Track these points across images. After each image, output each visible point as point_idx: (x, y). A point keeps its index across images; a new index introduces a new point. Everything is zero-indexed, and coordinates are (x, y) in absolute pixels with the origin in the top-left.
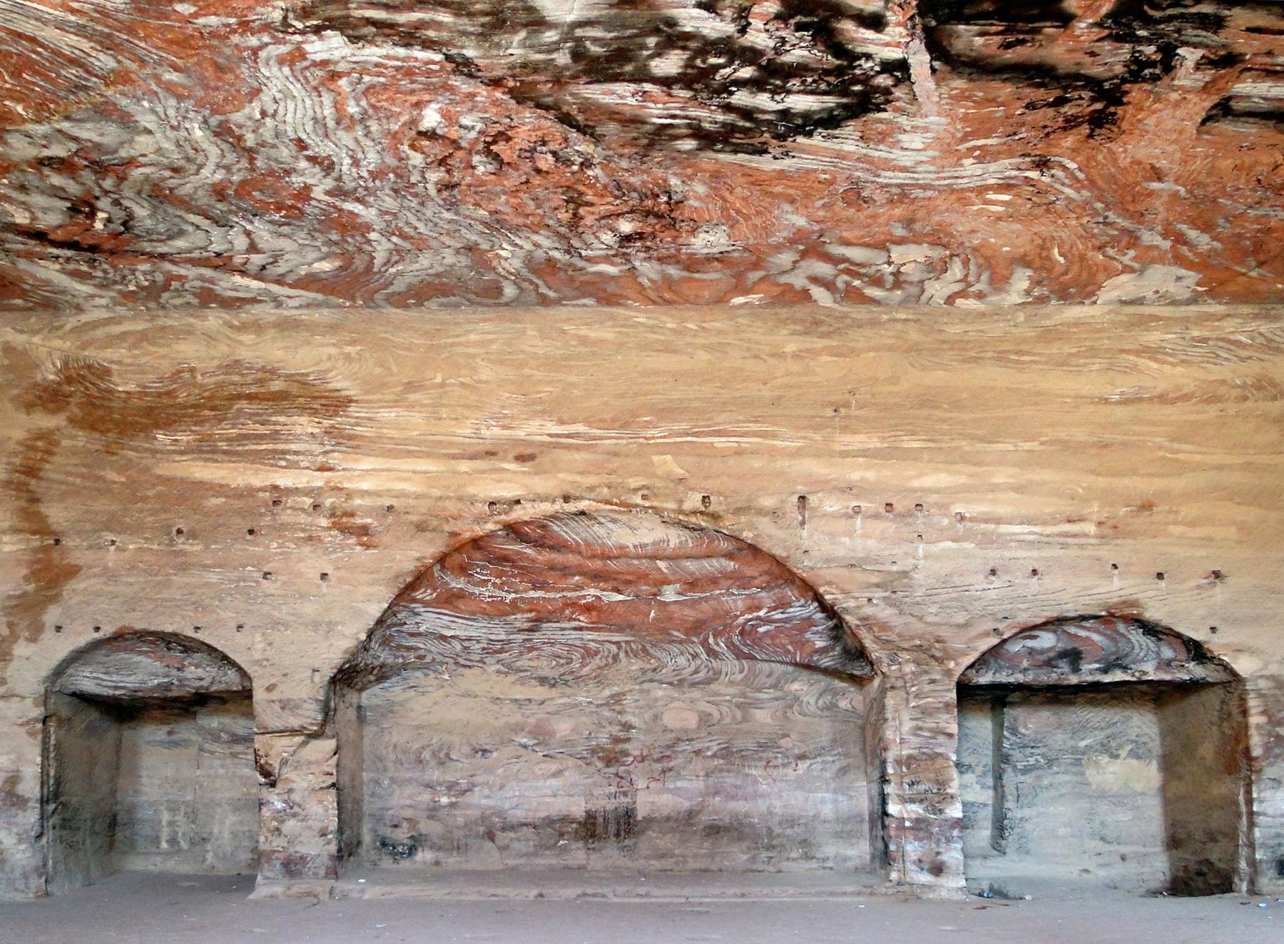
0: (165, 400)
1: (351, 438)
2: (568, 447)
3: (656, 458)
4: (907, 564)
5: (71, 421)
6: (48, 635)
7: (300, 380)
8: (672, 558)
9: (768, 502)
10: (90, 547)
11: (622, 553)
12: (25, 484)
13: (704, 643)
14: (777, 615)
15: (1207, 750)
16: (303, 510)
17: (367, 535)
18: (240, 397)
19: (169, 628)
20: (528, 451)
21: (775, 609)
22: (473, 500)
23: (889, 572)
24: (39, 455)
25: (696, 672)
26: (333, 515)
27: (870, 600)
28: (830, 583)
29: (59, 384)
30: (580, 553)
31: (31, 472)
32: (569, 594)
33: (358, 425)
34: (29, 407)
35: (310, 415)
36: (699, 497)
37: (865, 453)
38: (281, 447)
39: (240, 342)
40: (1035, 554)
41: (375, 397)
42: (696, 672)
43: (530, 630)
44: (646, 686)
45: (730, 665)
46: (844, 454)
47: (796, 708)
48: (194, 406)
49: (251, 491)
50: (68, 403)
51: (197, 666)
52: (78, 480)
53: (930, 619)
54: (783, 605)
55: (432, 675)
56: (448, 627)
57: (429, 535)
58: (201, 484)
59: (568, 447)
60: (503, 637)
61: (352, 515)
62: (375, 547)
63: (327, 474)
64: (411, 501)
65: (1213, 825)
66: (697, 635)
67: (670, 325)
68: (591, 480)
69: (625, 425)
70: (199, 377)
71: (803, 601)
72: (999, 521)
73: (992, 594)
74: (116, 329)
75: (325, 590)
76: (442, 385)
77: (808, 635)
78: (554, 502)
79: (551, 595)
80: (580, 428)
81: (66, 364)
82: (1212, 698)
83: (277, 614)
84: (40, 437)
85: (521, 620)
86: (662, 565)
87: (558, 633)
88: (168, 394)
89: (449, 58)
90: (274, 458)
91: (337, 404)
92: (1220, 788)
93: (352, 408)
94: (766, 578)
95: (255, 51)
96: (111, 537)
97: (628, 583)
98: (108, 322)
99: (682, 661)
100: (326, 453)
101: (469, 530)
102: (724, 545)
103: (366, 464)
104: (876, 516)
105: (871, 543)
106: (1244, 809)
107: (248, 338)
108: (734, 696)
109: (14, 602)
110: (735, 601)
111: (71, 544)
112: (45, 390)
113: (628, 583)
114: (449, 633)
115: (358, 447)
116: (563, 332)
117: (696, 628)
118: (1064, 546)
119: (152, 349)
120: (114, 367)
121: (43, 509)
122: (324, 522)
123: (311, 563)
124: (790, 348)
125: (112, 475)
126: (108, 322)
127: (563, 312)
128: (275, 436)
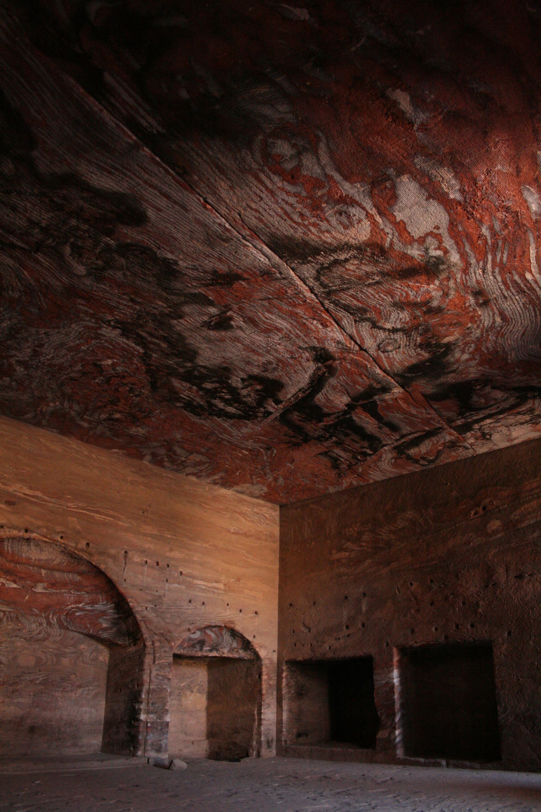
2: (32, 503)
3: (69, 518)
4: (161, 592)
8: (52, 569)
9: (113, 551)
11: (28, 562)
13: (47, 618)
14: (88, 608)
23: (155, 595)
25: (39, 633)
27: (146, 608)
28: (132, 597)
30: (6, 558)
37: (151, 536)
42: (39, 633)
44: (13, 639)
45: (56, 631)
47: (81, 658)
53: (167, 620)
54: (93, 603)
59: (32, 503)
66: (45, 612)
67: (86, 453)
68: (40, 523)
73: (189, 612)
77: (100, 620)
78: (20, 531)
80: (39, 494)
86: (43, 572)
89: (145, 354)
99: (34, 626)
102: (83, 568)
104: (152, 567)
105: (149, 580)
106: (256, 717)
108: (54, 649)
110: (69, 596)
117: (46, 608)
124: (129, 479)
127: (41, 431)
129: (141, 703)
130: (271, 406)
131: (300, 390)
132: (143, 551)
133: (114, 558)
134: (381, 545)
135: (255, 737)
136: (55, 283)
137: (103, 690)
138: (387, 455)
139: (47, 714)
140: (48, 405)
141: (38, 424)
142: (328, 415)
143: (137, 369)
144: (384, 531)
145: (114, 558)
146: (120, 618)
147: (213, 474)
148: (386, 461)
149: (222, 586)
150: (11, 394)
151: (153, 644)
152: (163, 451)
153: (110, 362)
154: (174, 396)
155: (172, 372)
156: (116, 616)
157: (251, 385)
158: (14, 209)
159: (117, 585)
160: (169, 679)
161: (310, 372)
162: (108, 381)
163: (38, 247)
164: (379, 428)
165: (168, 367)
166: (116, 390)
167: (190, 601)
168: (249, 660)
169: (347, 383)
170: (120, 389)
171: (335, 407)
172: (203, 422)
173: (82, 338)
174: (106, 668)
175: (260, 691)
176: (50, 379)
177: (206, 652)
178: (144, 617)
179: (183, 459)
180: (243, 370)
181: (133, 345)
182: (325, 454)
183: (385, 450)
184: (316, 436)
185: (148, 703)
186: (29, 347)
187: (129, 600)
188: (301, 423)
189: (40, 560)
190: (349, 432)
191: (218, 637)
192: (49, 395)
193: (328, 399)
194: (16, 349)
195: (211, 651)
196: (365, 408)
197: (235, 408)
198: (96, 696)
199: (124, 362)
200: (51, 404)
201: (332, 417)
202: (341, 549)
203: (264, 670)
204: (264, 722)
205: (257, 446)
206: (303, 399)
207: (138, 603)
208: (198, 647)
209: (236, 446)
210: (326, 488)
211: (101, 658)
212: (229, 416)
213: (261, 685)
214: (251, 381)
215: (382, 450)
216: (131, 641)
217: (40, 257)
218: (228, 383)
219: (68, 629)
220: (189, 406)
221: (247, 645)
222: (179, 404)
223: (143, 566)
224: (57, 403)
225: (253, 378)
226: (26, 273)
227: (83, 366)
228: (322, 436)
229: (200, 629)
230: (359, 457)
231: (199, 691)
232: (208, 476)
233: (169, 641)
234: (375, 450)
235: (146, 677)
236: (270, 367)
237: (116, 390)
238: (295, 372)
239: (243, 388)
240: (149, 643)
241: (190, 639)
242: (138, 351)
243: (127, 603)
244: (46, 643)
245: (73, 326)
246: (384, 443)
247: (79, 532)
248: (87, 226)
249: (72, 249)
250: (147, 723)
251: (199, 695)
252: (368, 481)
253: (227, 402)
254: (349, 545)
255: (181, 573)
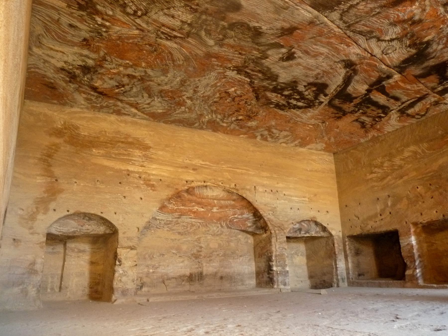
0: (96, 139)
1: (151, 158)
2: (205, 168)
3: (224, 173)
4: (275, 205)
5: (65, 141)
6: (51, 212)
7: (137, 140)
8: (219, 200)
9: (248, 187)
10: (68, 183)
11: (207, 197)
12: (47, 160)
13: (221, 224)
14: (240, 217)
15: (322, 253)
16: (136, 178)
17: (154, 187)
18: (119, 142)
19: (92, 212)
20: (195, 168)
21: (239, 215)
22: (182, 180)
24: (53, 151)
25: (218, 232)
26: (144, 180)
28: (261, 209)
29: (62, 129)
30: (197, 196)
31: (50, 156)
32: (190, 208)
33: (152, 154)
34: (51, 135)
35: (139, 150)
36: (234, 184)
37: (267, 177)
38: (130, 158)
39: (120, 126)
40: (298, 205)
41: (157, 147)
43: (178, 218)
44: (206, 235)
45: (226, 230)
46: (263, 177)
48: (106, 143)
49: (120, 171)
50: (64, 135)
51: (89, 225)
52: (66, 161)
54: (242, 214)
55: (149, 231)
56: (158, 216)
57: (170, 189)
58: (106, 167)
59: (205, 168)
60: (171, 220)
61: (150, 181)
62: (156, 191)
63: (143, 168)
64: (166, 179)
65: (325, 271)
68: (210, 177)
69: (218, 164)
70: (108, 134)
71: (248, 213)
72: (291, 196)
74: (82, 115)
75: (141, 203)
76: (175, 147)
77: (247, 222)
79: (186, 208)
80: (208, 163)
81: (65, 123)
82: (323, 241)
83: (127, 209)
84: (54, 145)
85: (176, 215)
86: (215, 201)
87: (186, 219)
88: (98, 137)
89: (251, 82)
90: (128, 161)
91: (147, 148)
92: (327, 262)
93: (151, 150)
94: (241, 206)
95: (216, 69)
96: (75, 180)
97: (206, 206)
98: (80, 112)
99: (215, 228)
100: (143, 162)
101: (181, 188)
102: (235, 197)
103: (154, 166)
104: (269, 193)
105: (269, 199)
107: (123, 125)
109: (39, 200)
110: (230, 212)
111: (61, 181)
112: (57, 130)
113: (206, 206)
114: (157, 218)
115: (152, 161)
116: (204, 137)
117: (219, 219)
118: (303, 203)
119: (93, 123)
120: (81, 126)
121: (52, 169)
122: (142, 182)
123: (138, 195)
124: (251, 149)
125: (77, 161)
126: (80, 112)
128: (129, 155)
129: (273, 261)
130: (322, 98)
131: (338, 86)
132: (263, 186)
133: (249, 190)
134: (396, 168)
135: (335, 277)
136: (199, 52)
137: (252, 257)
138: (394, 116)
139: (227, 270)
140: (205, 118)
141: (202, 128)
142: (356, 98)
143: (248, 91)
144: (396, 159)
145: (249, 190)
146: (256, 220)
147: (294, 141)
148: (394, 120)
149: (307, 199)
150: (186, 115)
151: (275, 232)
152: (266, 133)
153: (233, 89)
154: (269, 102)
155: (266, 89)
156: (254, 219)
157: (310, 88)
158: (173, 17)
159: (253, 204)
160: (286, 249)
161: (343, 75)
162: (233, 99)
163: (188, 35)
164: (388, 100)
165: (264, 87)
166: (238, 104)
167: (291, 209)
168: (327, 237)
169: (365, 78)
170: (240, 103)
171: (360, 93)
172: (286, 113)
173: (217, 79)
174: (253, 246)
175: (335, 253)
176: (204, 104)
177: (303, 234)
178: (268, 219)
179: (278, 135)
180: (304, 81)
181: (244, 78)
182: (357, 120)
183: (393, 113)
184: (350, 111)
185: (276, 262)
186: (191, 89)
187: (260, 211)
188: (341, 105)
189: (213, 196)
190: (370, 106)
191: (308, 226)
192: (205, 112)
193: (355, 89)
194: (185, 91)
195: (305, 234)
196: (378, 90)
197: (303, 103)
198: (250, 260)
199: (241, 88)
200: (207, 117)
201: (358, 99)
202: (372, 173)
203: (335, 241)
204: (339, 269)
205: (317, 122)
206: (340, 91)
207: (264, 211)
208: (298, 232)
209: (305, 123)
210: (359, 140)
211: (249, 241)
212: (300, 108)
213: (335, 249)
214: (310, 86)
215: (391, 113)
216: (263, 231)
217: (190, 40)
218: (297, 90)
219: (231, 228)
220: (278, 106)
221: (324, 229)
222: (272, 106)
223: (264, 193)
224: (209, 116)
225: (310, 84)
226: (184, 50)
227: (220, 94)
228: (353, 111)
229: (298, 223)
230: (377, 119)
231: (301, 255)
232: (292, 142)
233: (283, 230)
234: (386, 114)
235: (273, 249)
236: (319, 76)
237: (238, 104)
238: (334, 76)
239: (305, 91)
240: (273, 232)
241: (294, 228)
242: (247, 81)
243: (259, 212)
244: (222, 236)
245: (212, 73)
246: (391, 109)
247: (230, 180)
248: (211, 18)
249: (205, 32)
250: (277, 271)
251: (301, 257)
252: (384, 132)
253: (297, 100)
254: (376, 170)
255: (285, 195)
